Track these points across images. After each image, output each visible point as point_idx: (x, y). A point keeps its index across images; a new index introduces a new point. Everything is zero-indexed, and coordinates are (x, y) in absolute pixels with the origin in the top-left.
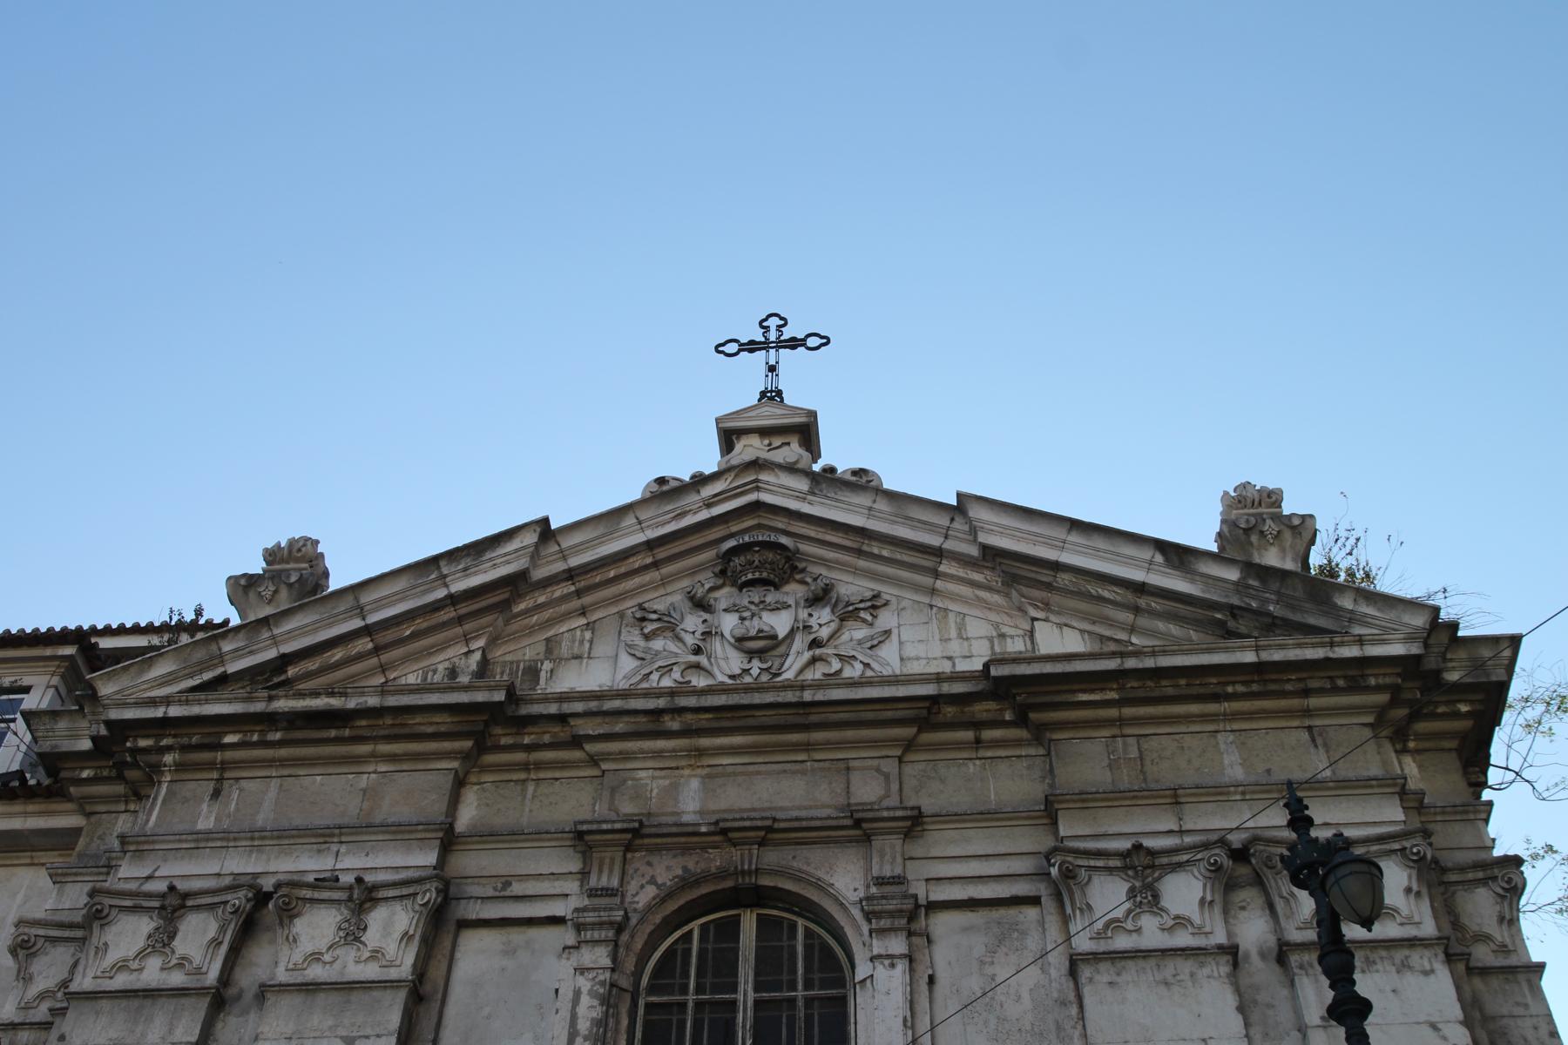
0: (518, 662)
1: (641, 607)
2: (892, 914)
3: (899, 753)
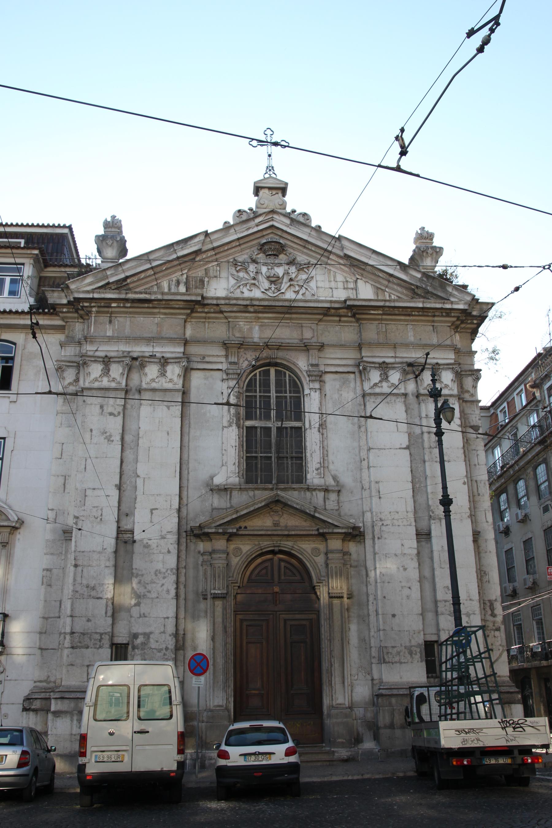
0: (197, 277)
1: (235, 260)
2: (315, 376)
3: (317, 322)
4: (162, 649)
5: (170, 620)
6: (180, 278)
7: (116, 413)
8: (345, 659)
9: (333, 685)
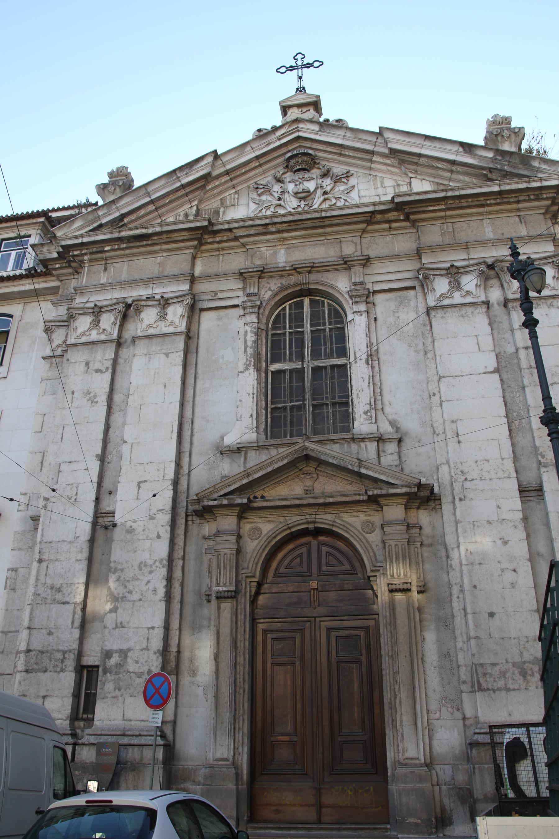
0: (211, 209)
1: (256, 183)
2: (360, 296)
3: (360, 234)
4: (143, 673)
5: (156, 630)
6: (189, 211)
7: (103, 369)
8: (417, 686)
9: (398, 727)
